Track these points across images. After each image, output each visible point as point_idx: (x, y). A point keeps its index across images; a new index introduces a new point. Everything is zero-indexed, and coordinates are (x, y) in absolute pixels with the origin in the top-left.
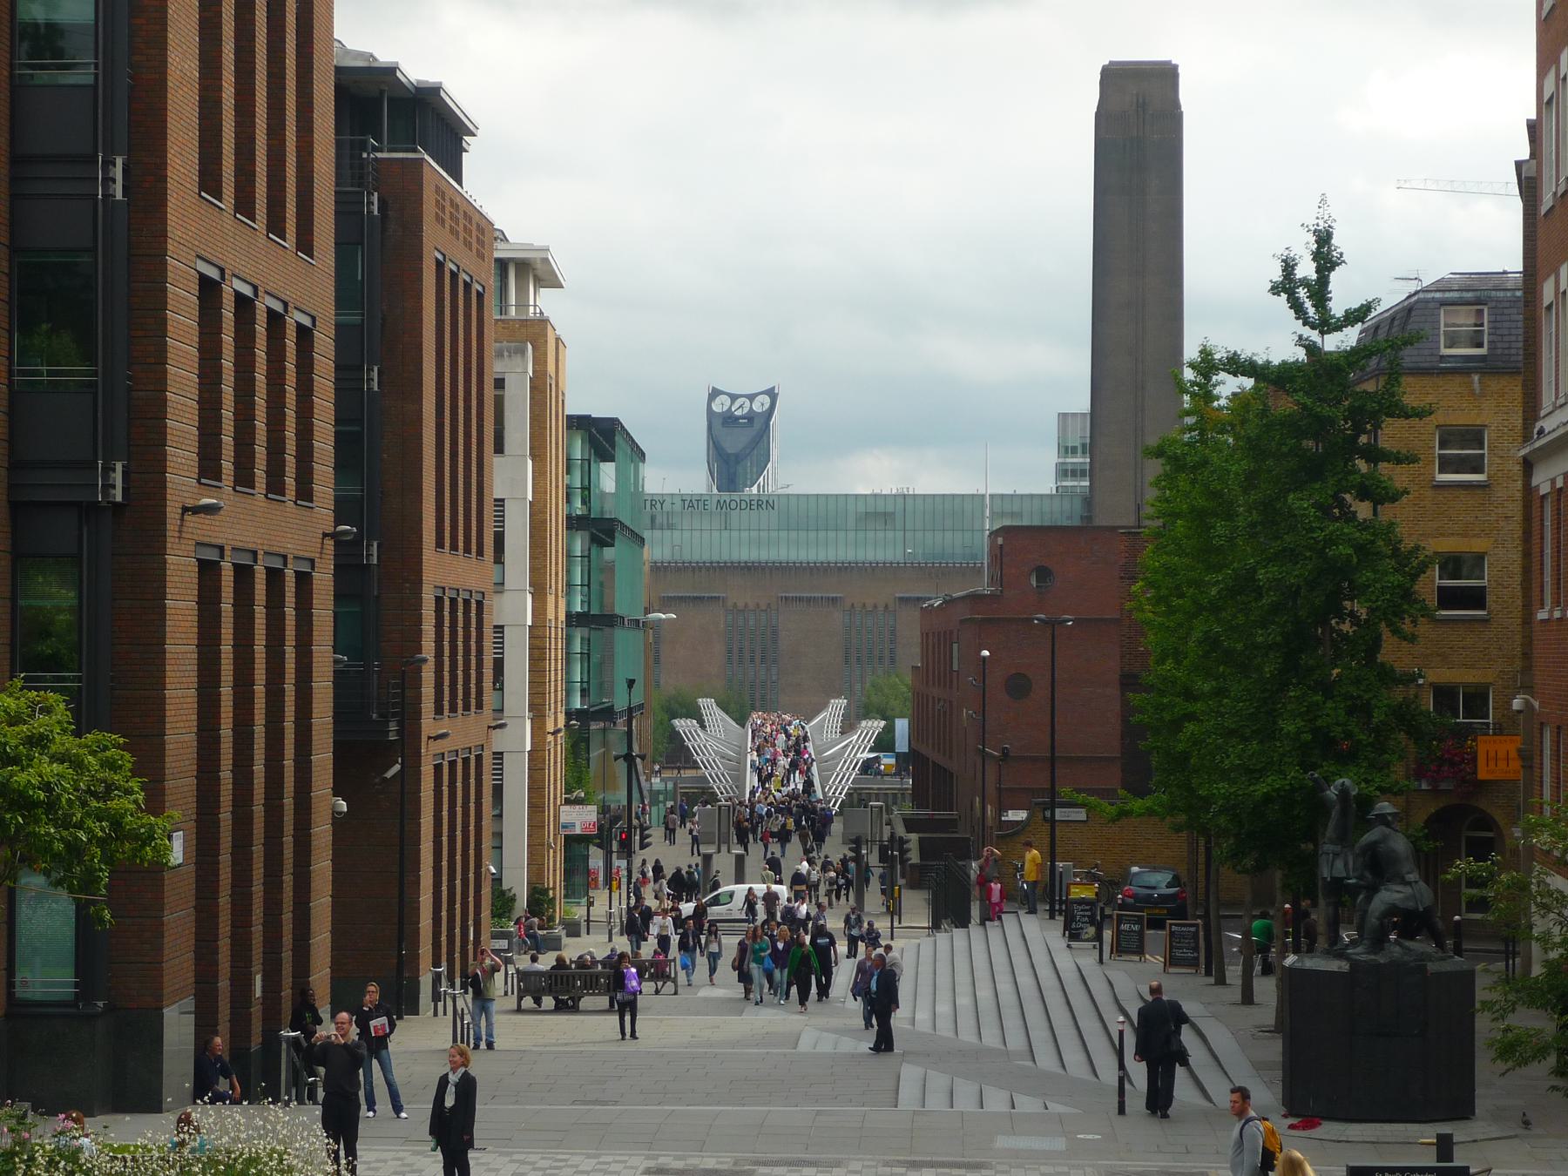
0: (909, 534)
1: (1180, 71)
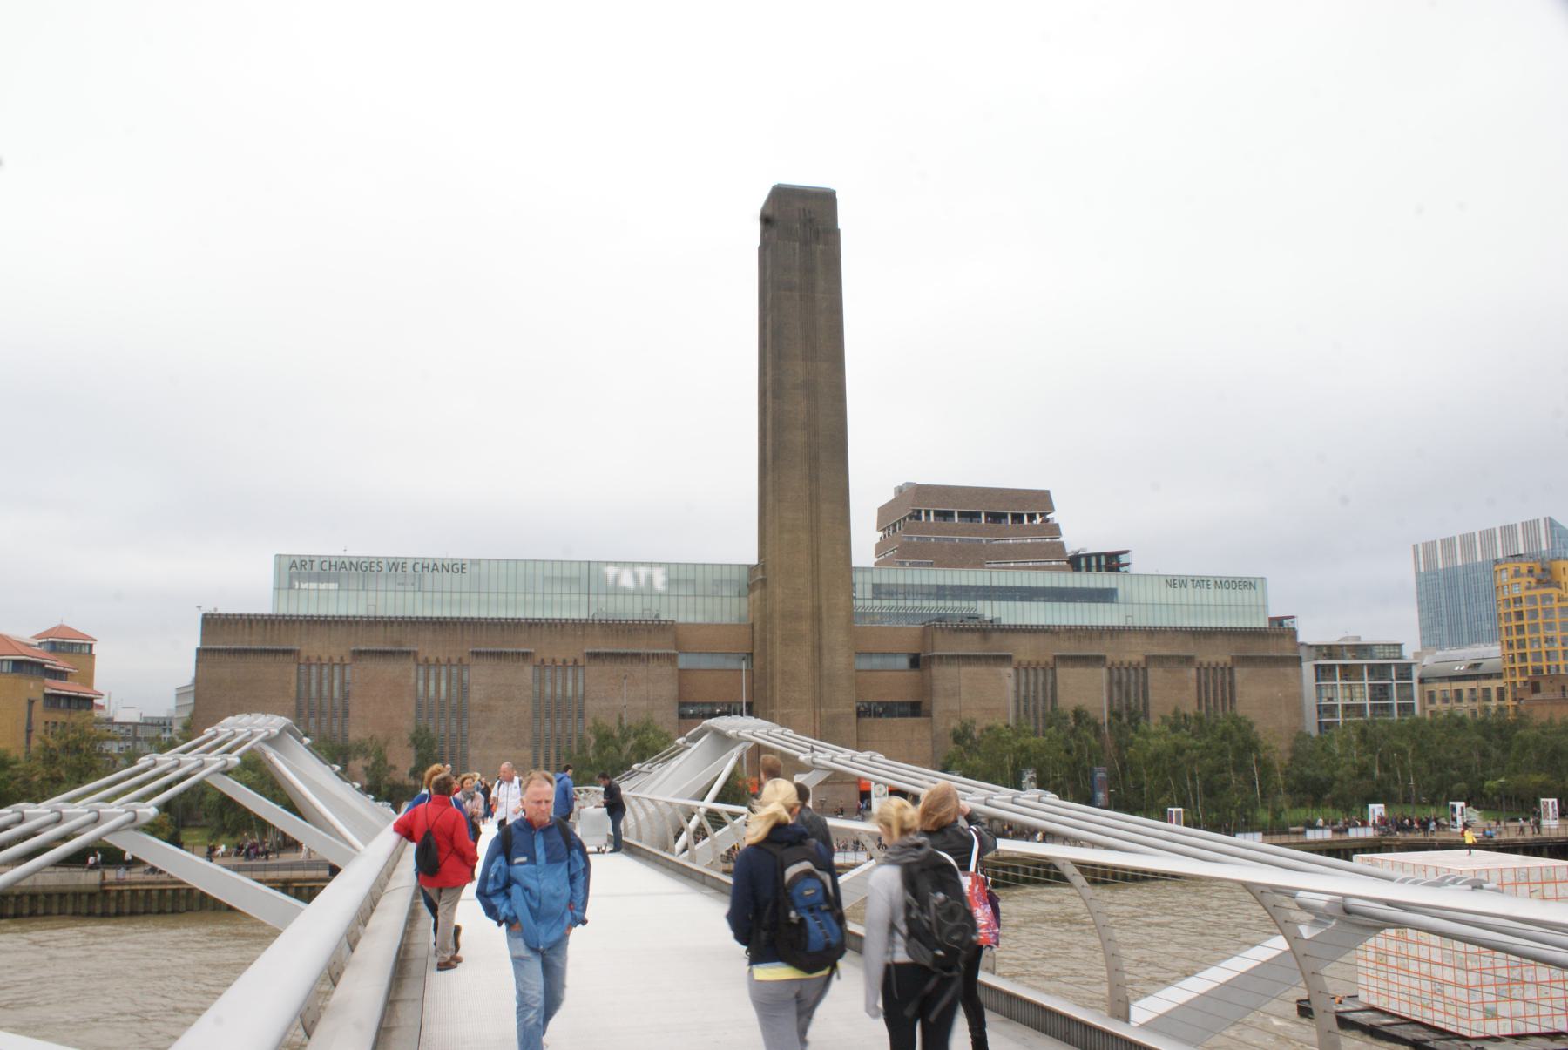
0: (593, 598)
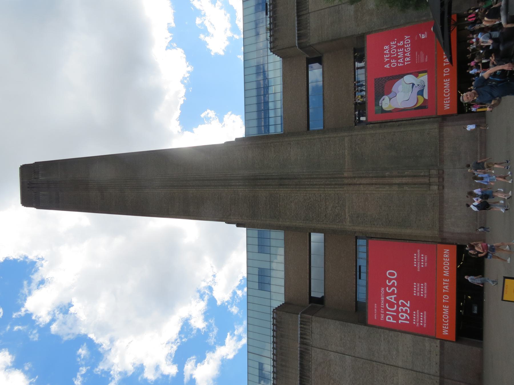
1: (31, 161)
